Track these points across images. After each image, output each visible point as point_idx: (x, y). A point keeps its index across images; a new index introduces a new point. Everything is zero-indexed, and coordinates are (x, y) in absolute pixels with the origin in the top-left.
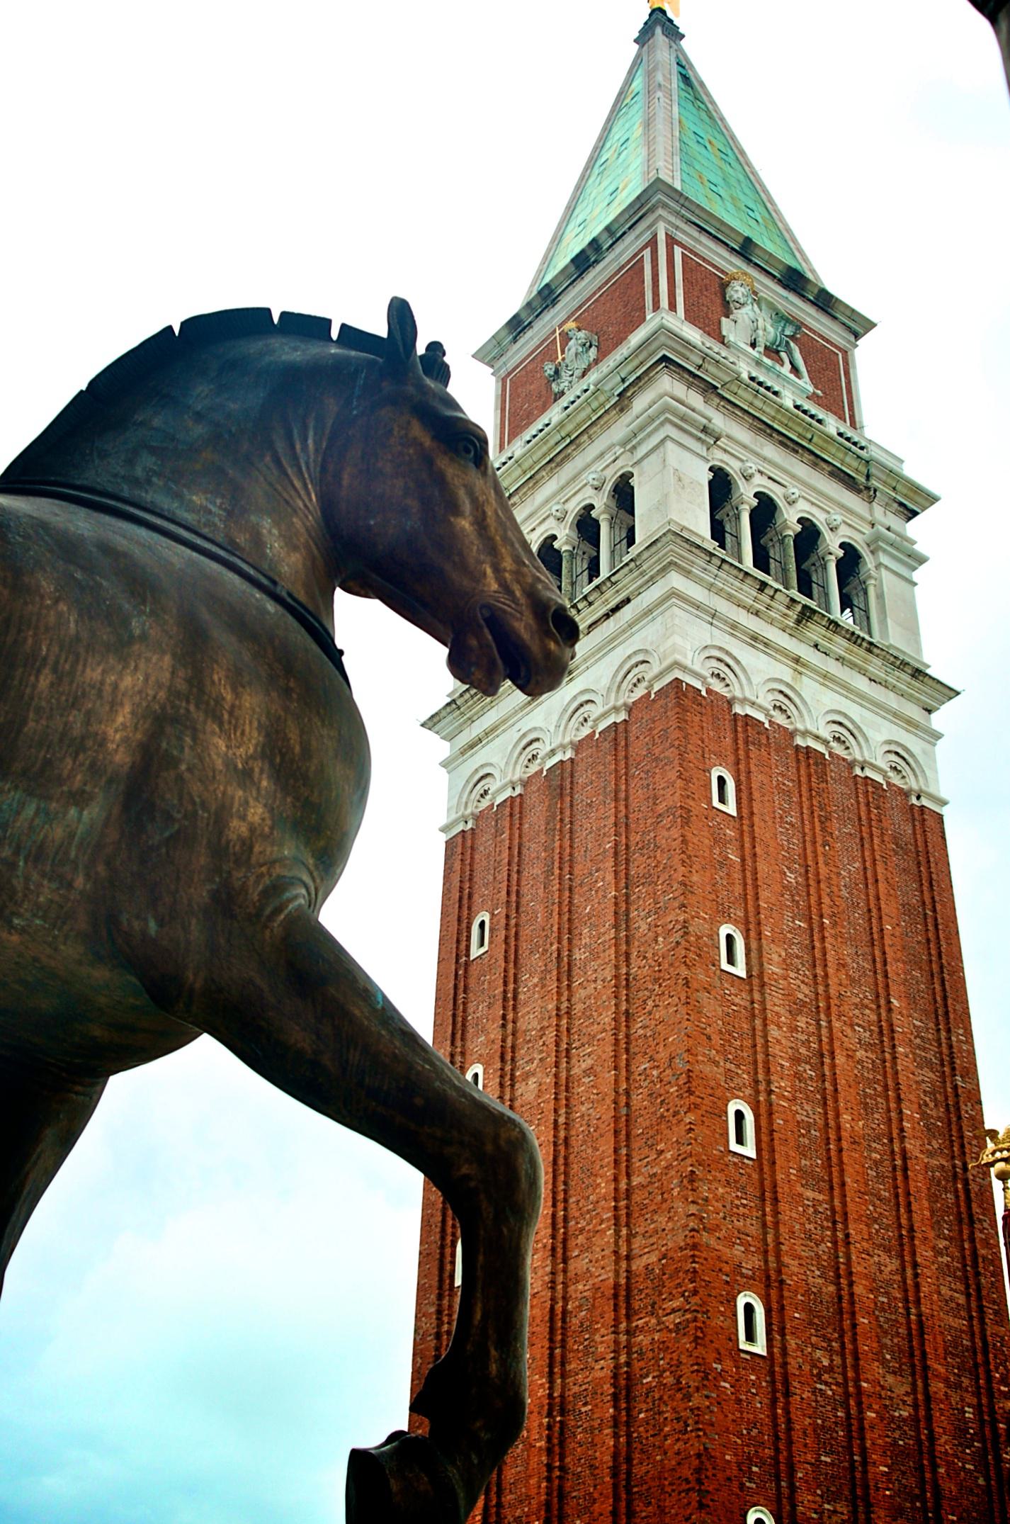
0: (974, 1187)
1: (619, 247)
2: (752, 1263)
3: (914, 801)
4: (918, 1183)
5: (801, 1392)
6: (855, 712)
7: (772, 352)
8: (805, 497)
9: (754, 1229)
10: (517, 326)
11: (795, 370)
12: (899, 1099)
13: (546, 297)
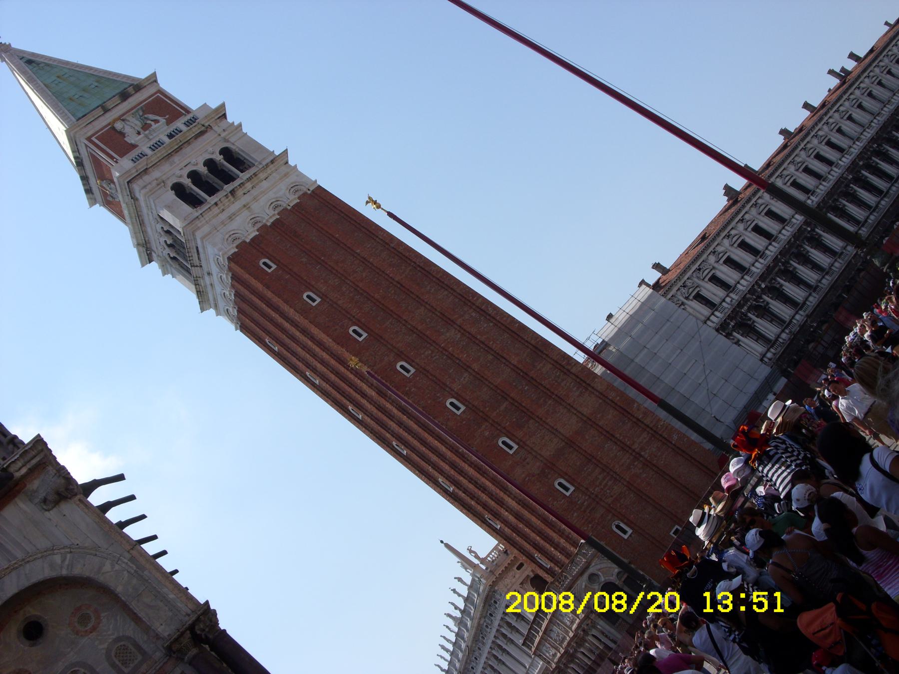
0: (421, 265)
1: (81, 151)
7: (146, 127)
8: (196, 157)
10: (88, 191)
11: (156, 121)
13: (84, 179)
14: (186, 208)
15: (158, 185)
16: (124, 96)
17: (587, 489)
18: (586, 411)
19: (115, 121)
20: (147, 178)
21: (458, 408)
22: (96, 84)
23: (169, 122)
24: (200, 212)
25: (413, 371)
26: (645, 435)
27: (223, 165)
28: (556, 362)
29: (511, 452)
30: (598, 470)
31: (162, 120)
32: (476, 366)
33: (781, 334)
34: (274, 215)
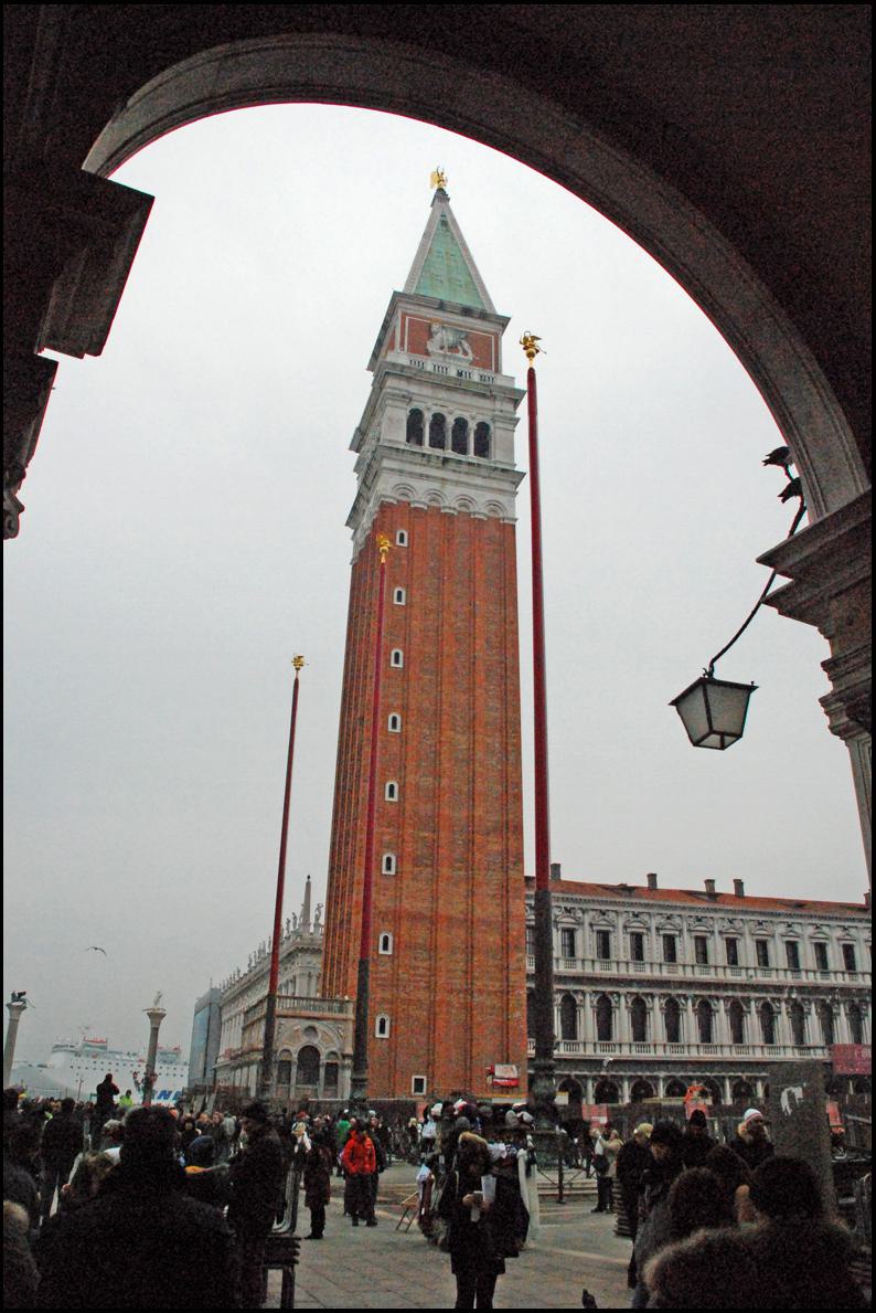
2: (397, 703)
3: (501, 522)
4: (480, 667)
5: (412, 743)
6: (471, 493)
8: (455, 408)
9: (399, 691)
11: (465, 353)
12: (474, 638)
14: (400, 435)
15: (404, 397)
16: (467, 312)
17: (399, 966)
18: (478, 912)
19: (437, 321)
20: (403, 385)
21: (391, 795)
22: (462, 283)
23: (474, 363)
24: (407, 448)
25: (398, 730)
26: (498, 984)
27: (469, 435)
28: (507, 850)
29: (384, 872)
30: (425, 964)
31: (471, 356)
32: (445, 782)
33: (817, 1047)
34: (454, 509)
